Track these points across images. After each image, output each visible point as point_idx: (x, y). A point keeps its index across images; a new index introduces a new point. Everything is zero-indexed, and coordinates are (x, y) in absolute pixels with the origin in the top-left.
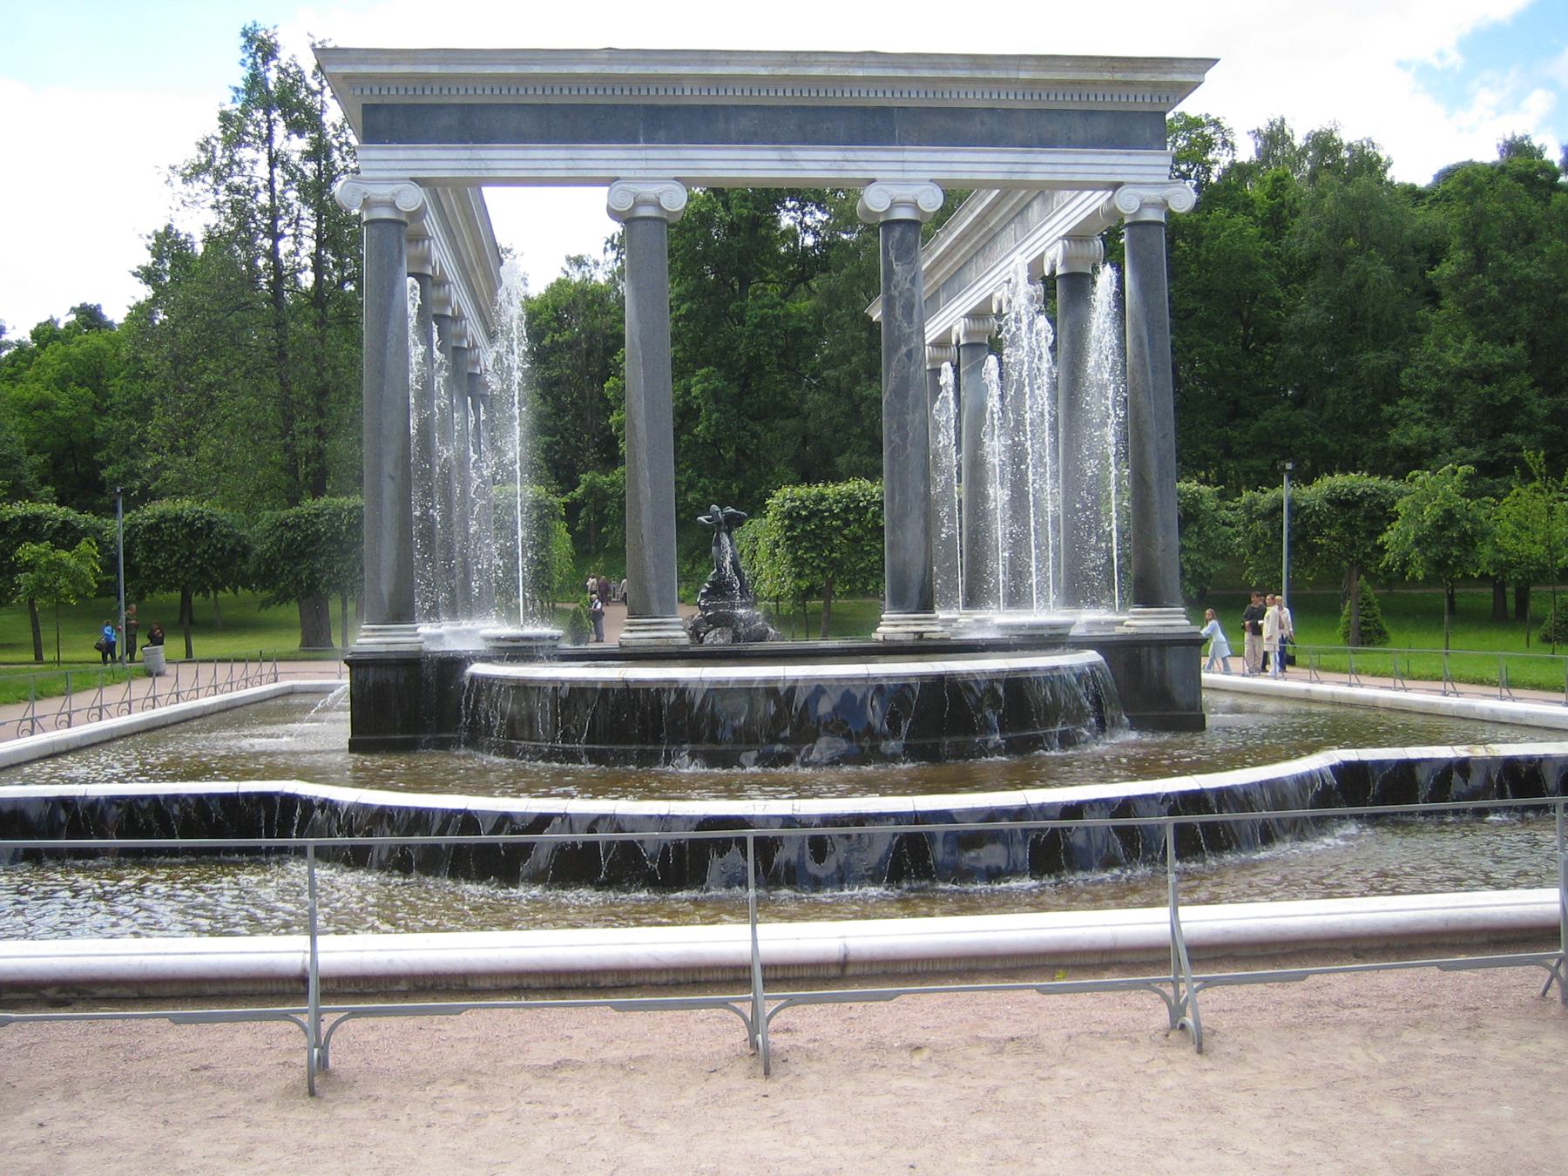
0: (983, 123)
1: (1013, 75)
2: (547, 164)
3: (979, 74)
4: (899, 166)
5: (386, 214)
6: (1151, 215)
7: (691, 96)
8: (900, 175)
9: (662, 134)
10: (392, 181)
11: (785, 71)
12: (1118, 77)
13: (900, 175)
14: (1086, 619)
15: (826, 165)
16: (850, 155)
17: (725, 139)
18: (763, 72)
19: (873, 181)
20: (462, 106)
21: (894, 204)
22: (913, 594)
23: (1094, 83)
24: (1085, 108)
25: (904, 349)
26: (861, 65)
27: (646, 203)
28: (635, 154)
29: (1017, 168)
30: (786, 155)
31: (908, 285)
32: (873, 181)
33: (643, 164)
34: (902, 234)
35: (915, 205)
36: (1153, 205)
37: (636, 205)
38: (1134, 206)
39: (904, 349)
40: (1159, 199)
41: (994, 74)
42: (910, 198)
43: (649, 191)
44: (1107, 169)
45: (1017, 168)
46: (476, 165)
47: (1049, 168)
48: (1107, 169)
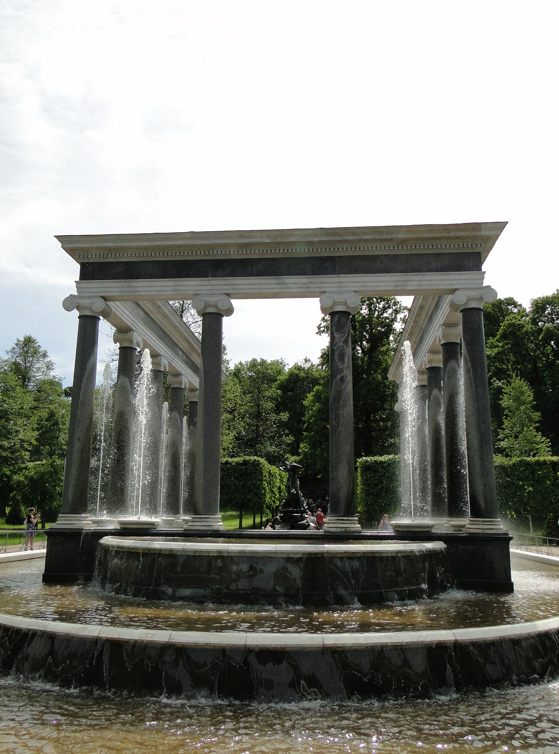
0: (382, 262)
1: (394, 236)
2: (164, 289)
3: (377, 237)
4: (338, 285)
5: (88, 313)
6: (473, 305)
7: (234, 255)
8: (338, 289)
9: (220, 272)
10: (90, 297)
11: (278, 240)
12: (452, 234)
13: (338, 289)
14: (443, 524)
15: (301, 285)
16: (312, 280)
17: (251, 274)
18: (267, 241)
19: (325, 292)
20: (127, 263)
21: (335, 304)
22: (342, 507)
23: (440, 238)
24: (436, 252)
25: (339, 377)
26: (316, 236)
27: (211, 306)
28: (206, 283)
29: (399, 283)
30: (280, 281)
31: (341, 344)
32: (325, 292)
33: (210, 287)
34: (339, 318)
35: (346, 304)
36: (475, 299)
37: (205, 307)
38: (464, 299)
39: (339, 377)
40: (478, 297)
41: (385, 237)
42: (343, 301)
43: (212, 300)
44: (449, 282)
45: (399, 283)
46: (131, 289)
47: (417, 283)
48: (449, 282)
